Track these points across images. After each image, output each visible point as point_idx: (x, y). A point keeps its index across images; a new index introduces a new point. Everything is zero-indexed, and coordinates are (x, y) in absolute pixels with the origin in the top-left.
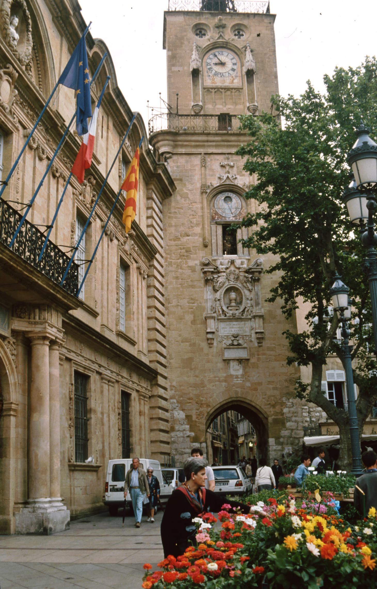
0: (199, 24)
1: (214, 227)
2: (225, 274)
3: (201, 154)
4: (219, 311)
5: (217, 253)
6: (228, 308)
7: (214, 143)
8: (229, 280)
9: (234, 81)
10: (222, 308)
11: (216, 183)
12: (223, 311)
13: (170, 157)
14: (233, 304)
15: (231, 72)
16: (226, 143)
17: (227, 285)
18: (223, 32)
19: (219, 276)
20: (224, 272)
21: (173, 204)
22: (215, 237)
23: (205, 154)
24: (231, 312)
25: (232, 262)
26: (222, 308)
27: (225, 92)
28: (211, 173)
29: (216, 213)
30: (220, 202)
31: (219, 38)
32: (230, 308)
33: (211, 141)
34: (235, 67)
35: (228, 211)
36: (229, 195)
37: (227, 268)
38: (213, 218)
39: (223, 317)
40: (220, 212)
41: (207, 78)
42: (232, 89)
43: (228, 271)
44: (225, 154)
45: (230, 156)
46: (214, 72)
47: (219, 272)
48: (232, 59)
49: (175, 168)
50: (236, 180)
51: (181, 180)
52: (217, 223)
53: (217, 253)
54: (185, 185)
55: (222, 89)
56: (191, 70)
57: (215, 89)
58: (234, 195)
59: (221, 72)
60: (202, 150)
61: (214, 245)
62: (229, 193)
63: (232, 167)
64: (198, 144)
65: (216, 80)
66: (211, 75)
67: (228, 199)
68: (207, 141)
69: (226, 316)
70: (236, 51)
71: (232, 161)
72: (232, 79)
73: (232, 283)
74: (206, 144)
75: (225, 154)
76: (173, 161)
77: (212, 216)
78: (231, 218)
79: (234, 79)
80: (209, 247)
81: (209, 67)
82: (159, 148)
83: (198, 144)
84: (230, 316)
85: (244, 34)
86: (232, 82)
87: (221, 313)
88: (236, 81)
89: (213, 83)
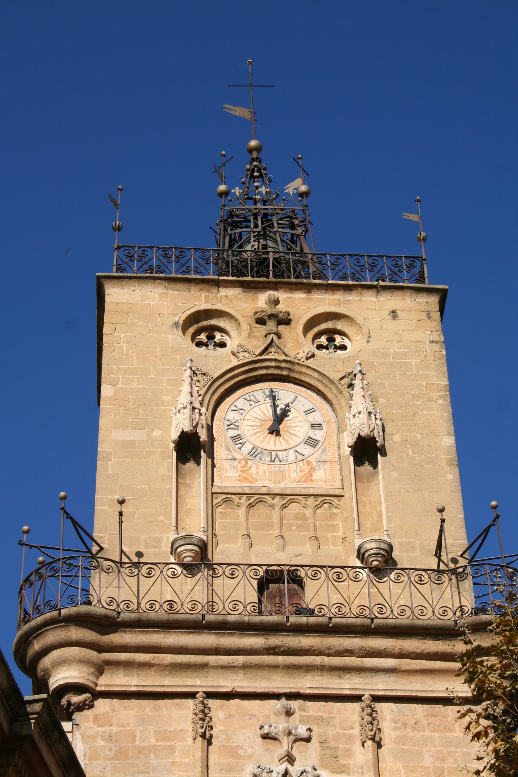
0: (208, 314)
3: (192, 695)
7: (240, 659)
9: (316, 475)
15: (307, 450)
18: (279, 336)
23: (210, 695)
27: (284, 507)
28: (227, 760)
31: (265, 350)
34: (318, 435)
41: (226, 465)
42: (307, 496)
44: (277, 696)
45: (295, 704)
46: (247, 448)
48: (307, 412)
49: (101, 743)
55: (274, 495)
56: (175, 435)
57: (250, 495)
59: (271, 447)
60: (198, 682)
65: (253, 470)
66: (239, 457)
71: (303, 720)
72: (307, 469)
74: (211, 659)
75: (277, 696)
76: (96, 719)
79: (313, 469)
81: (232, 433)
82: (47, 675)
85: (346, 342)
86: (309, 477)
88: (318, 475)
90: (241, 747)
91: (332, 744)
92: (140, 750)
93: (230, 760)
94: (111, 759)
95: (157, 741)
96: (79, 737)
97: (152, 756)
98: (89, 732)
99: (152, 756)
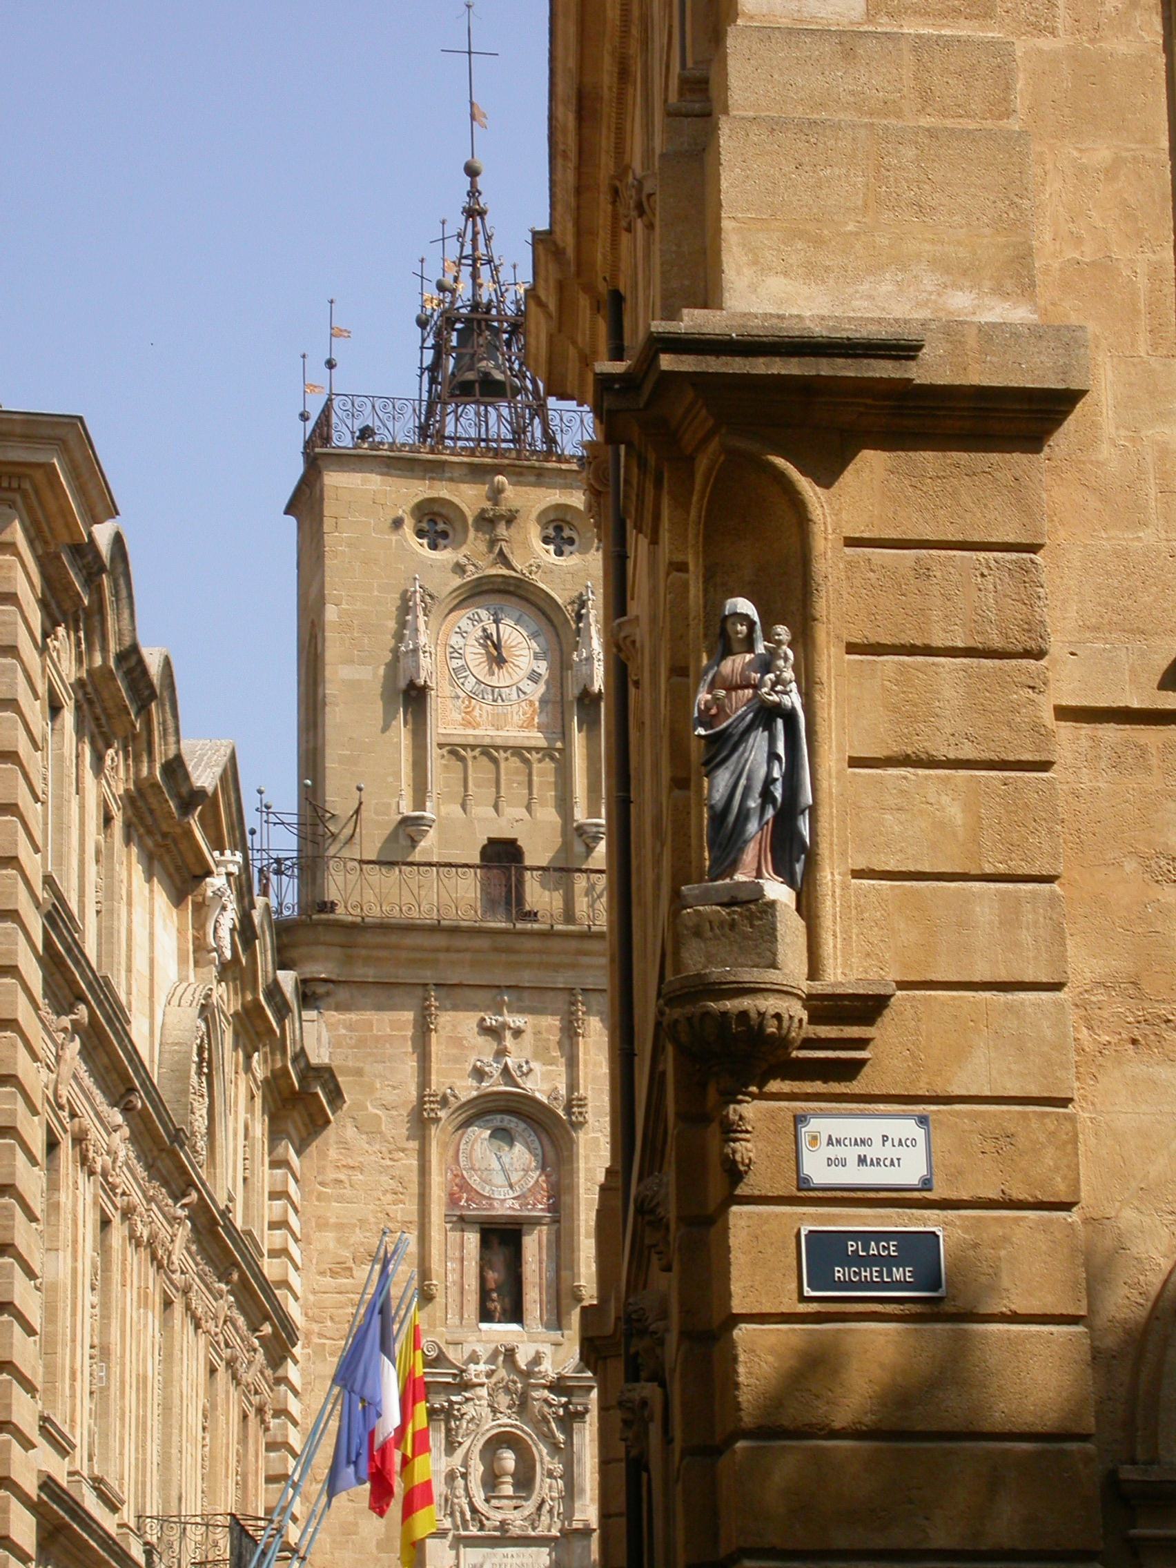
1: (454, 1236)
2: (483, 1392)
4: (462, 1513)
5: (462, 1318)
6: (487, 1500)
7: (468, 956)
8: (494, 1411)
10: (471, 1504)
11: (467, 1089)
12: (474, 1510)
13: (328, 994)
14: (508, 1490)
16: (504, 957)
17: (490, 1426)
19: (467, 1400)
20: (482, 1385)
21: (333, 1153)
22: (456, 1266)
24: (498, 1516)
25: (510, 1354)
26: (471, 1504)
29: (464, 1186)
30: (477, 1147)
32: (494, 1502)
33: (458, 951)
35: (499, 1179)
36: (505, 1124)
37: (489, 1375)
38: (453, 1201)
39: (474, 1531)
40: (474, 1181)
43: (494, 1380)
47: (467, 1386)
49: (343, 1031)
50: (530, 1076)
51: (359, 1072)
52: (462, 1222)
53: (462, 1318)
54: (371, 1089)
58: (522, 1126)
61: (453, 1291)
62: (507, 1118)
63: (518, 1033)
64: (418, 955)
67: (503, 1135)
68: (448, 950)
69: (482, 1527)
70: (549, 612)
73: (508, 1421)
74: (442, 956)
77: (451, 1195)
78: (509, 1203)
80: (440, 1299)
83: (418, 955)
84: (495, 1529)
87: (468, 1516)
89: (468, 724)
90: (465, 1038)
91: (545, 1035)
92: (377, 1039)
93: (454, 1051)
94: (353, 1048)
95: (392, 1030)
96: (324, 1025)
97: (388, 1045)
98: (333, 1020)
99: (388, 1045)
